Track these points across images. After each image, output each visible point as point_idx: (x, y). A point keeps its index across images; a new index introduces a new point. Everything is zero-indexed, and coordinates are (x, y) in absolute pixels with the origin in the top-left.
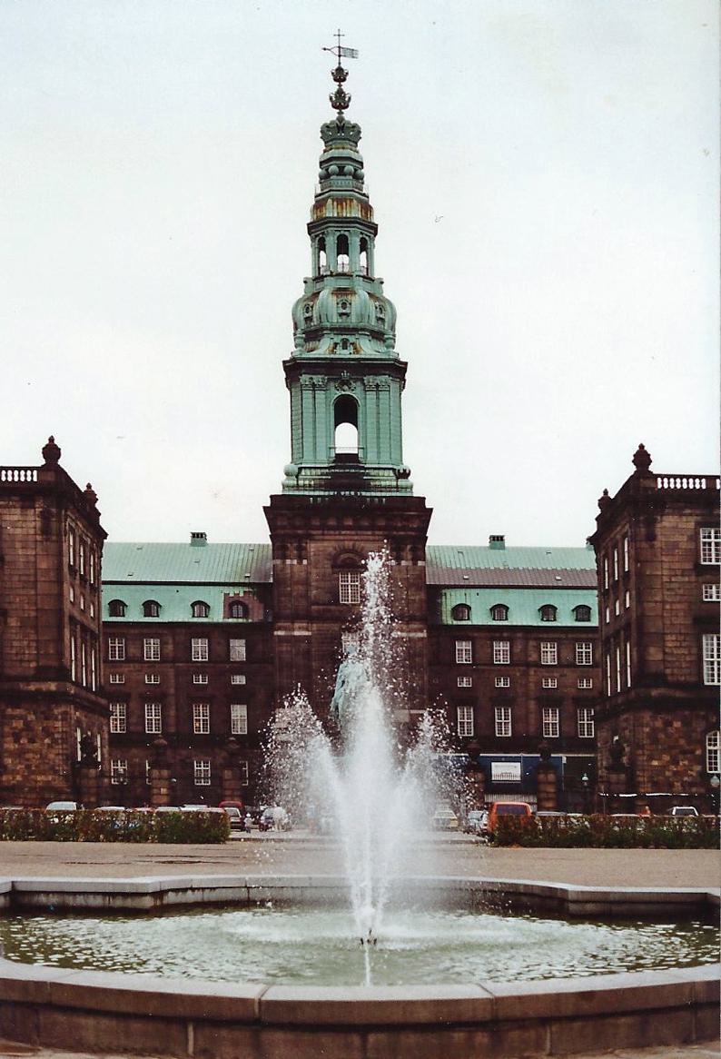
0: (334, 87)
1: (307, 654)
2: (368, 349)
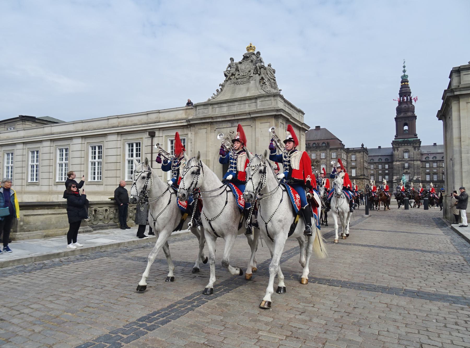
0: (403, 69)
1: (399, 167)
2: (409, 114)
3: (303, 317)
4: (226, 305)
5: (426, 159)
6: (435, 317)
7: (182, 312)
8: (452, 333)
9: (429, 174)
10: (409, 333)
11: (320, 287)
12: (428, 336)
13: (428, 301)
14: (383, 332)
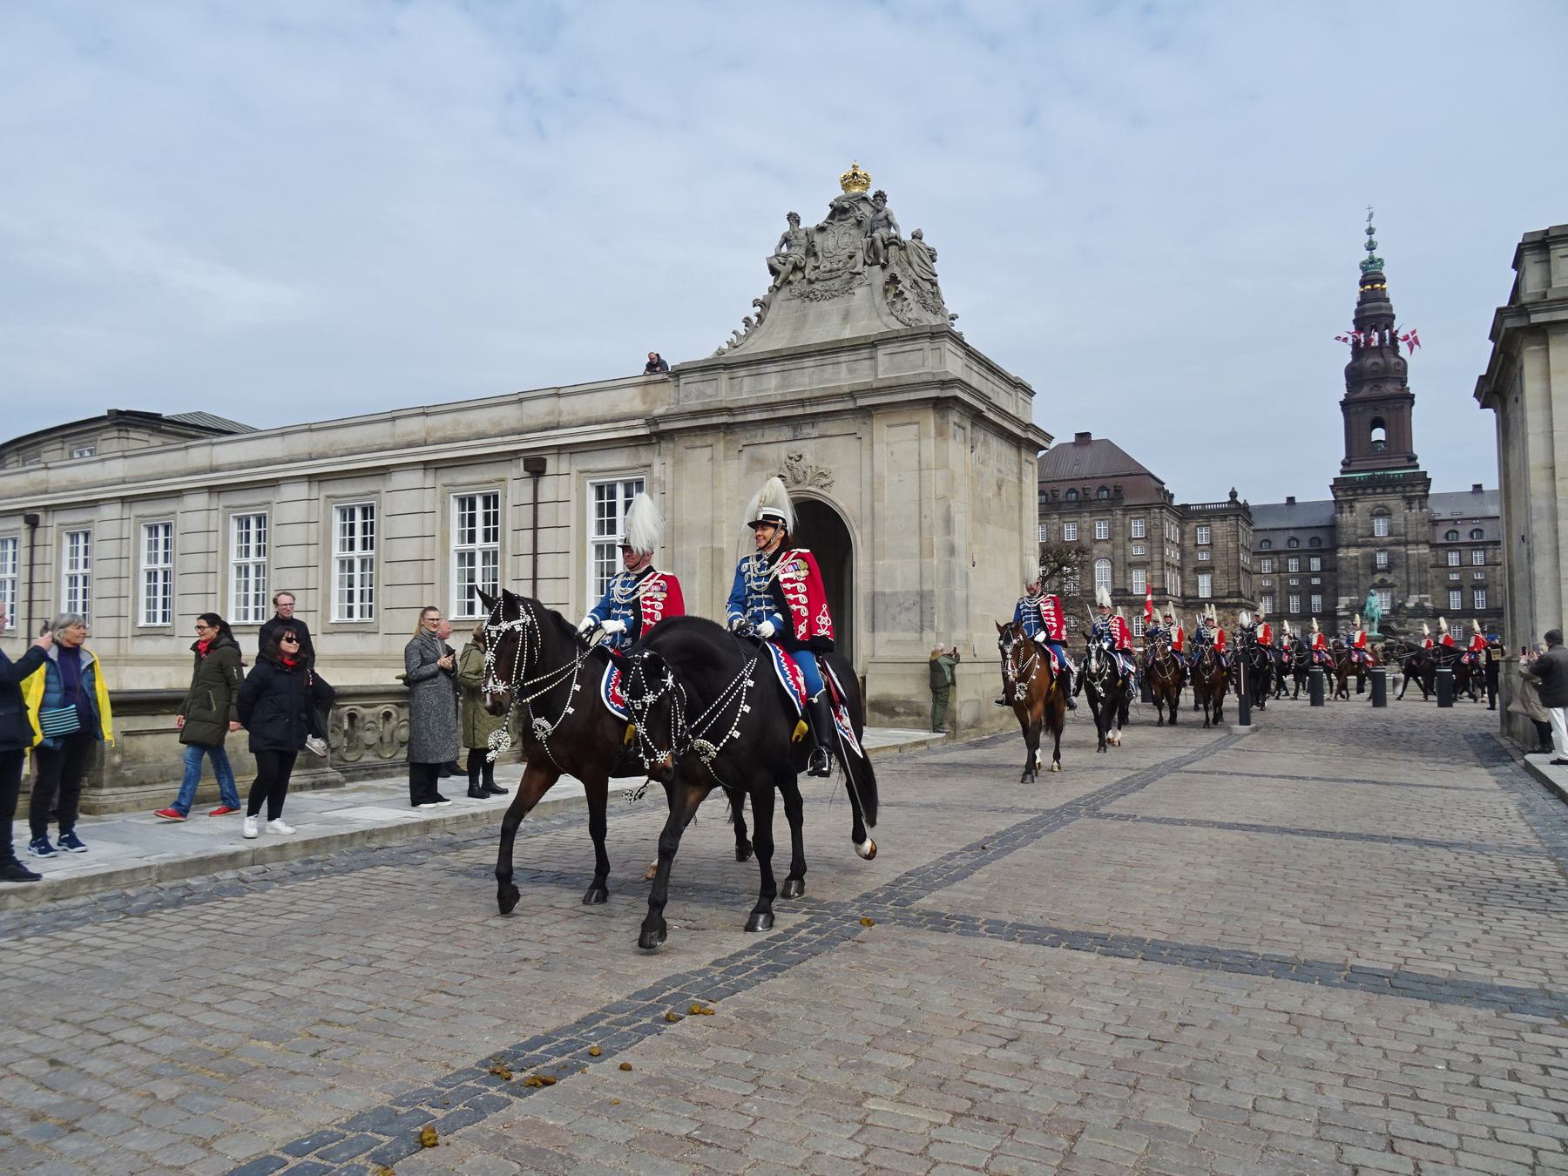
0: (1366, 238)
1: (1356, 566)
2: (1390, 388)
3: (1011, 1054)
4: (765, 1018)
5: (1447, 536)
6: (1445, 1055)
7: (624, 1038)
8: (1495, 1104)
9: (1457, 587)
10: (1352, 1104)
11: (1073, 959)
12: (1416, 1115)
13: (1427, 1003)
14: (1270, 1102)
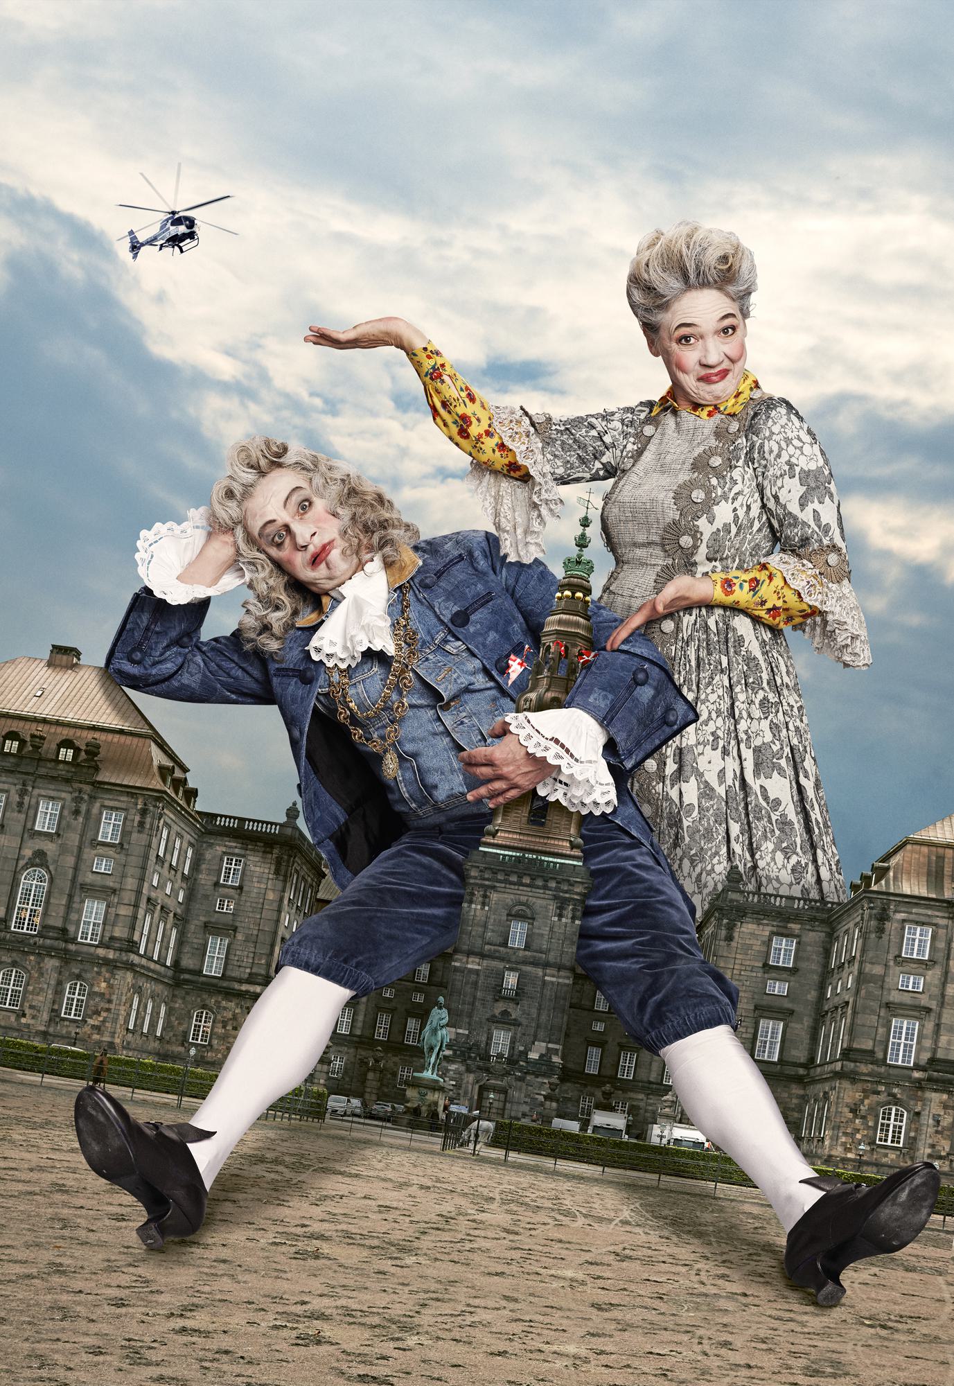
1: (476, 983)
